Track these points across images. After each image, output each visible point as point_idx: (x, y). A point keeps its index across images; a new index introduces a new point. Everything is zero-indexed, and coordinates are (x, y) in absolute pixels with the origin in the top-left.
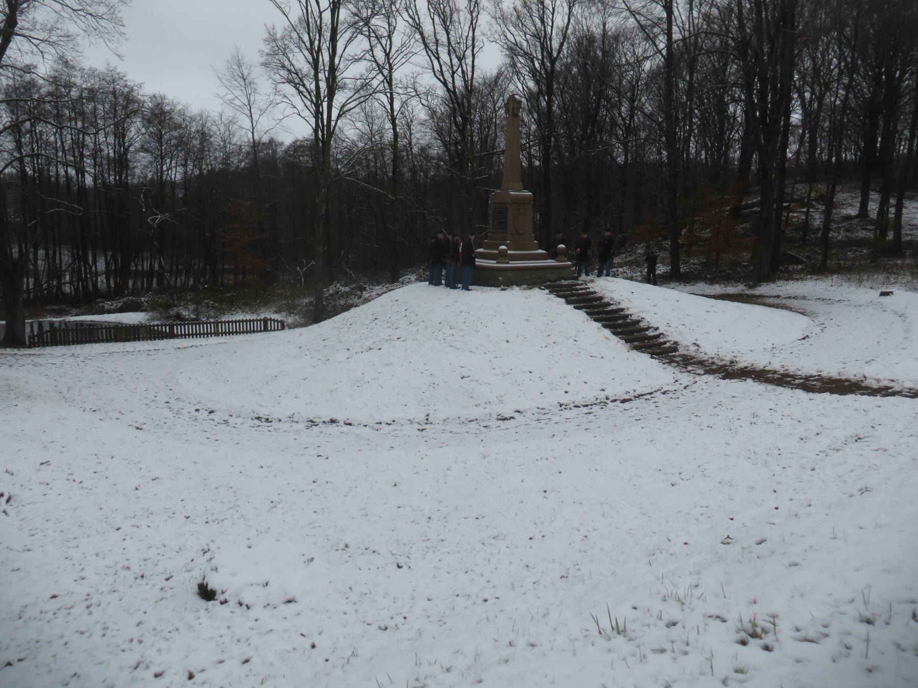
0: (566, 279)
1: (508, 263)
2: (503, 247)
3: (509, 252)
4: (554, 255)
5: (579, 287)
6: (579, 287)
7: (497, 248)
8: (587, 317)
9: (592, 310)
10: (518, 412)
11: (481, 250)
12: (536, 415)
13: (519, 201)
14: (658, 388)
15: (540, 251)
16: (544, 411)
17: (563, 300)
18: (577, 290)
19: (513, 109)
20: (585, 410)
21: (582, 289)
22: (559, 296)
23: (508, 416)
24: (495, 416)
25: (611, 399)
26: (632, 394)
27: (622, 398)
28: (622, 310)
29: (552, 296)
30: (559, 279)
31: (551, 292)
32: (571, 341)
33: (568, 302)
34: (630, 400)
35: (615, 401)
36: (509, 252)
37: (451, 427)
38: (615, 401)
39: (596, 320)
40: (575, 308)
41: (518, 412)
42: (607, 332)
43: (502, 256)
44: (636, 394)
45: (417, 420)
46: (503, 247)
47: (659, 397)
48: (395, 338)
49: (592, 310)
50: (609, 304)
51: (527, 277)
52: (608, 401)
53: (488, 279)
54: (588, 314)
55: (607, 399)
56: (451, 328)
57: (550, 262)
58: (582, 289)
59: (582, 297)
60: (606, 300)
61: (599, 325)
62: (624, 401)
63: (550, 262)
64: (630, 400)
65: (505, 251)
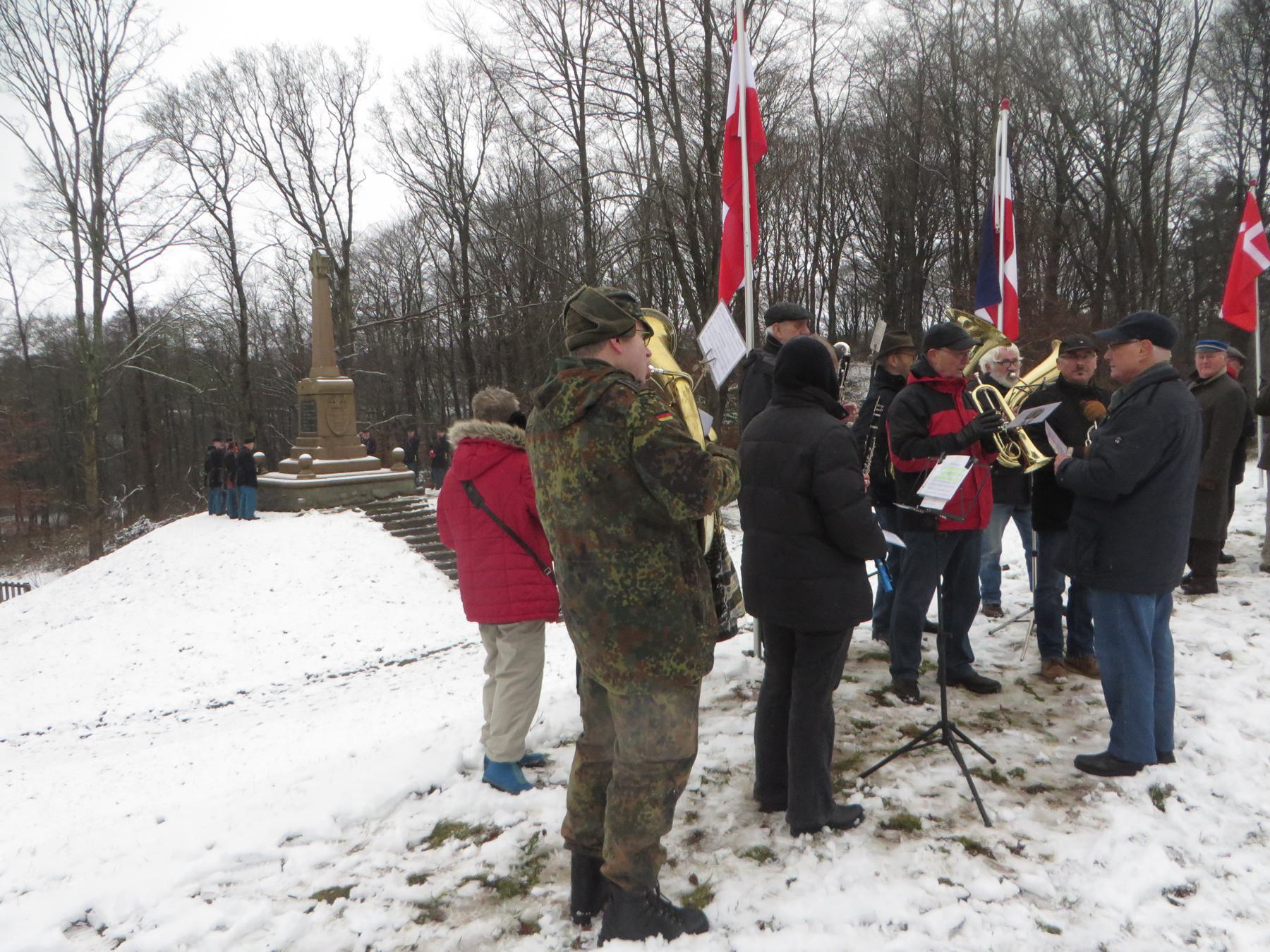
0: (403, 494)
1: (313, 477)
2: (305, 456)
3: (316, 462)
4: (385, 463)
6: (413, 505)
7: (296, 457)
10: (243, 693)
11: (287, 461)
12: (268, 694)
13: (332, 393)
14: (460, 640)
16: (280, 688)
17: (380, 525)
18: (410, 509)
20: (341, 680)
21: (416, 508)
22: (376, 520)
23: (224, 702)
24: (205, 703)
25: (386, 661)
26: (420, 651)
27: (401, 660)
30: (395, 495)
32: (368, 582)
33: (386, 528)
34: (415, 660)
35: (392, 663)
36: (316, 462)
37: (132, 728)
38: (392, 663)
39: (418, 551)
40: (393, 535)
41: (243, 693)
42: (429, 566)
43: (305, 468)
44: (425, 652)
45: (84, 723)
46: (305, 456)
47: (457, 651)
48: (117, 599)
51: (344, 495)
52: (381, 666)
53: (281, 500)
54: (409, 541)
55: (381, 661)
56: (200, 577)
57: (385, 472)
58: (416, 508)
61: (419, 556)
62: (402, 664)
63: (385, 472)
64: (415, 660)
65: (310, 461)
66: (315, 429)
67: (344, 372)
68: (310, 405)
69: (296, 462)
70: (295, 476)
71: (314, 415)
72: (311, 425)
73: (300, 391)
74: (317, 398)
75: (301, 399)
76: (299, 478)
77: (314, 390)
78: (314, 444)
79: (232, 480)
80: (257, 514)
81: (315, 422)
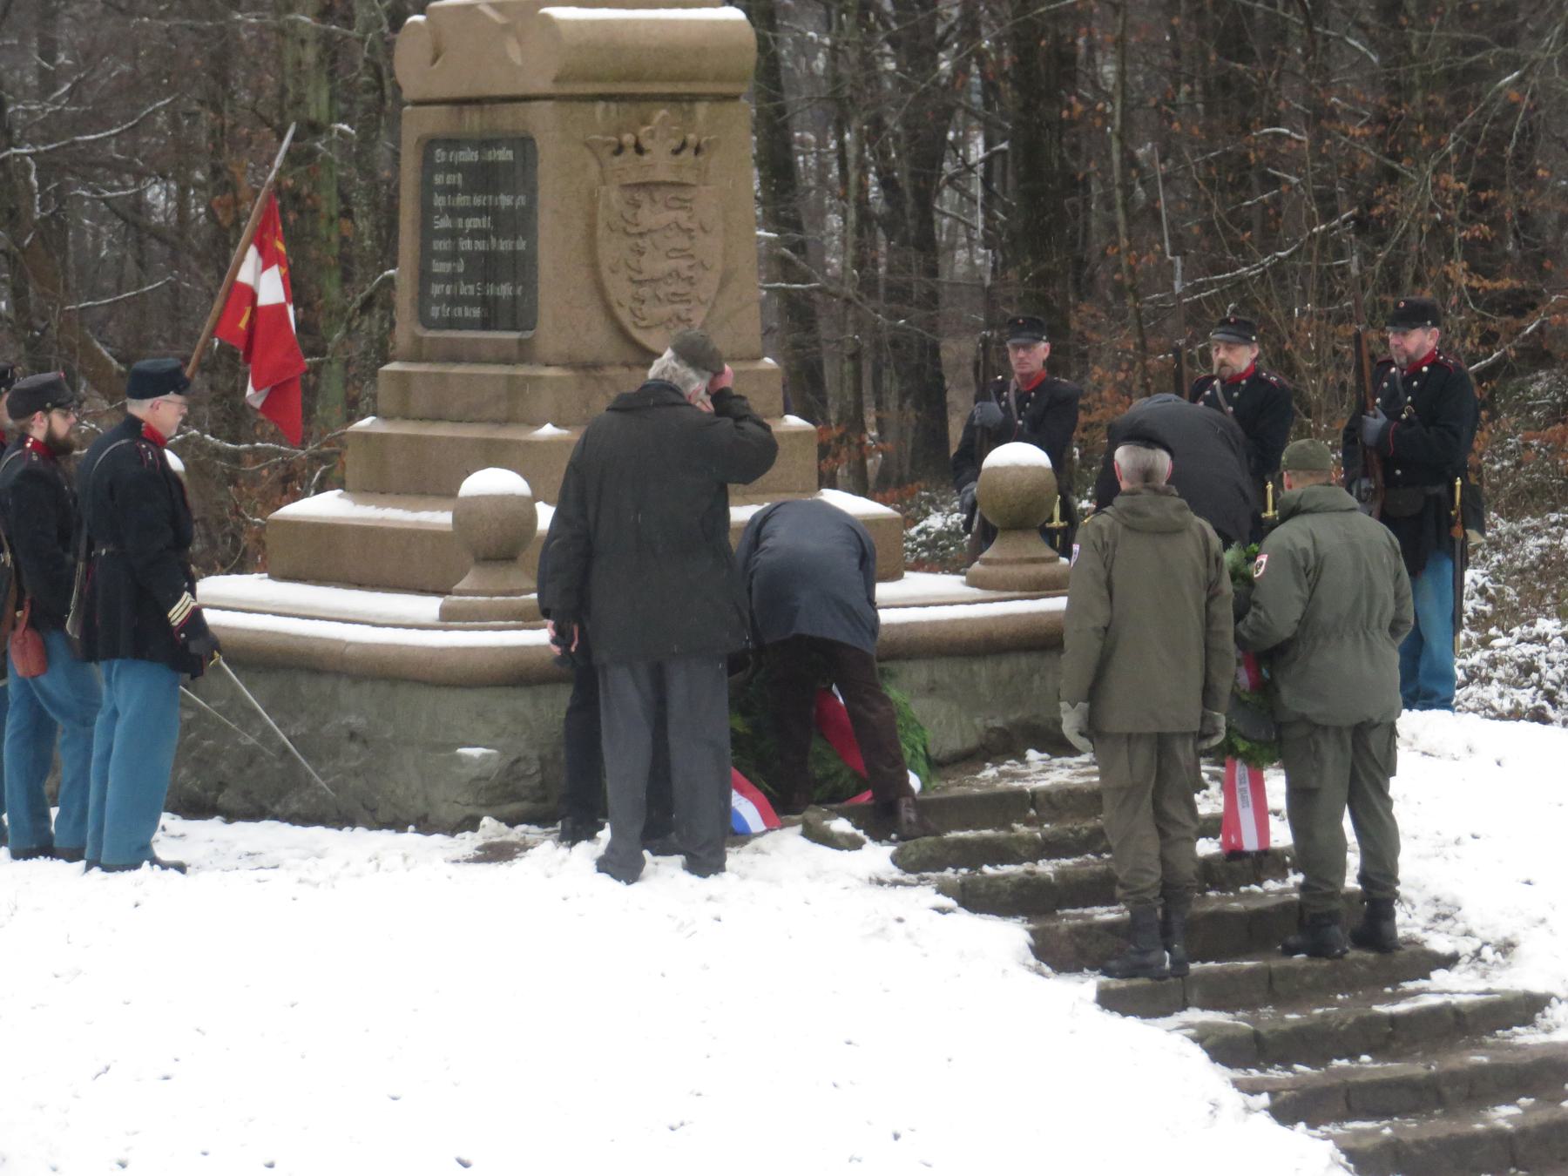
2: (493, 482)
7: (441, 488)
8: (1216, 1080)
17: (1012, 935)
22: (975, 899)
28: (1529, 1007)
29: (924, 897)
31: (913, 865)
33: (1056, 954)
46: (493, 482)
54: (1223, 1050)
66: (517, 315)
68: (492, 166)
69: (441, 518)
70: (429, 607)
71: (521, 223)
72: (497, 291)
73: (412, 69)
74: (542, 121)
75: (417, 125)
76: (449, 618)
78: (515, 406)
79: (46, 620)
80: (176, 835)
81: (521, 267)
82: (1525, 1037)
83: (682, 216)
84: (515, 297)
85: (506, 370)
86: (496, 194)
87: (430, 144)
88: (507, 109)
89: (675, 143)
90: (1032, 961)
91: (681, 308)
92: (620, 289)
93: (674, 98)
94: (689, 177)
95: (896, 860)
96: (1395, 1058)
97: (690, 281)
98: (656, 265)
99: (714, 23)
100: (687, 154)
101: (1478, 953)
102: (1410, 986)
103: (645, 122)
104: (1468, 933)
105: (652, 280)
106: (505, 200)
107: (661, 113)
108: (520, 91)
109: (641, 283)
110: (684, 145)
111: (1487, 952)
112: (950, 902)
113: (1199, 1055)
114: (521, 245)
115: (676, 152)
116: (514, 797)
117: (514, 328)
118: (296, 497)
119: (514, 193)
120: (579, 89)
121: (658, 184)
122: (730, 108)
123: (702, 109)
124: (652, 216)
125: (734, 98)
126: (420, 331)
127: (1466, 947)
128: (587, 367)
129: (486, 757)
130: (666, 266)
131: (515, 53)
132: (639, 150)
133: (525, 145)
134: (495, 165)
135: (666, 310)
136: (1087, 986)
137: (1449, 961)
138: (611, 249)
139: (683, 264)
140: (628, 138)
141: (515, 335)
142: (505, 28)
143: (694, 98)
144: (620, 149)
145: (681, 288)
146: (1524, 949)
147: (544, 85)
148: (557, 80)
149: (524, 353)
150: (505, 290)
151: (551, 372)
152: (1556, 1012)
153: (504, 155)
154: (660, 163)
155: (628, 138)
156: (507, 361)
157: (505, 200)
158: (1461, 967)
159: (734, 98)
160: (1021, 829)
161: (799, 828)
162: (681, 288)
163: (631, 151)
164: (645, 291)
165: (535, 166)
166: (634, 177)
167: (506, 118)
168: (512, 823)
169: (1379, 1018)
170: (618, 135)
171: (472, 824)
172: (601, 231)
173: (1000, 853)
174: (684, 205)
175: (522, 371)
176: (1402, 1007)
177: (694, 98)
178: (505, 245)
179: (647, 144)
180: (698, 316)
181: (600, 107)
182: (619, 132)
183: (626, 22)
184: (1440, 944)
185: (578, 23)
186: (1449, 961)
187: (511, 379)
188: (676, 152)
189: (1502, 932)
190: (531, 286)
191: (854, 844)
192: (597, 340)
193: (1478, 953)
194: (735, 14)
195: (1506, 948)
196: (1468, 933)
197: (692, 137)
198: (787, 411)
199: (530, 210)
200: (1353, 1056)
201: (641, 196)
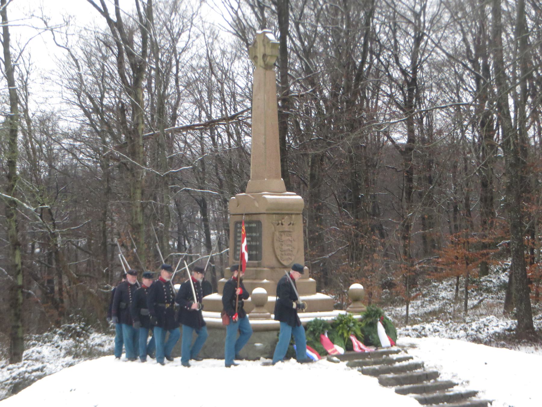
5: (394, 356)
9: (425, 396)
13: (281, 212)
15: (320, 296)
17: (375, 380)
18: (394, 361)
19: (264, 56)
21: (400, 360)
22: (364, 372)
28: (474, 394)
33: (384, 383)
40: (397, 392)
49: (425, 396)
50: (451, 385)
59: (403, 375)
60: (444, 378)
67: (289, 188)
71: (259, 239)
74: (263, 219)
77: (258, 207)
82: (474, 399)
83: (290, 238)
84: (256, 254)
85: (255, 269)
86: (252, 233)
87: (236, 223)
88: (258, 216)
89: (289, 223)
90: (379, 384)
91: (290, 256)
92: (278, 252)
93: (288, 214)
94: (291, 230)
95: (348, 365)
96: (451, 402)
97: (292, 251)
98: (285, 248)
99: (296, 199)
100: (291, 226)
101: (462, 383)
102: (450, 389)
103: (283, 219)
104: (460, 379)
105: (284, 251)
106: (254, 234)
107: (286, 217)
108: (258, 212)
109: (282, 251)
110: (290, 224)
111: (464, 383)
112: (360, 373)
113: (417, 402)
114: (258, 243)
115: (289, 225)
116: (266, 353)
117: (257, 260)
118: (210, 293)
119: (256, 233)
120: (268, 212)
121: (285, 231)
122: (298, 216)
123: (293, 216)
124: (285, 238)
125: (299, 214)
126: (234, 261)
127: (460, 382)
128: (272, 268)
129: (260, 346)
130: (287, 248)
131: (257, 205)
132: (282, 224)
133: (259, 223)
134: (252, 227)
135: (287, 257)
136: (391, 390)
137: (458, 384)
138: (277, 244)
139: (290, 248)
140: (280, 222)
141: (256, 262)
142: (254, 200)
143: (292, 214)
144: (278, 224)
145: (290, 252)
146: (471, 383)
147: (265, 212)
148: (267, 210)
149: (259, 265)
150: (254, 253)
151: (266, 269)
152: (479, 394)
153: (254, 225)
154: (286, 227)
155: (280, 222)
156: (255, 267)
157: (254, 234)
158: (459, 385)
159: (299, 214)
160: (367, 360)
161: (326, 359)
162: (290, 252)
163: (280, 225)
164: (283, 253)
165: (261, 227)
166: (281, 230)
167: (255, 218)
168: (266, 358)
169: (447, 396)
170: (278, 221)
171: (258, 359)
172: (275, 240)
173: (366, 364)
174: (290, 236)
175: (259, 269)
176: (451, 393)
177: (292, 214)
178: (254, 243)
179: (283, 223)
180: (293, 258)
181: (274, 216)
182: (278, 221)
183: (280, 198)
184: (455, 381)
185: (271, 199)
186: (458, 384)
187: (256, 270)
188: (289, 225)
189: (466, 379)
190: (261, 252)
191: (338, 362)
192: (274, 263)
193: (462, 383)
194: (299, 197)
195: (468, 382)
196: (460, 379)
197: (292, 222)
198: (310, 277)
199: (260, 236)
200: (443, 402)
201: (282, 234)
